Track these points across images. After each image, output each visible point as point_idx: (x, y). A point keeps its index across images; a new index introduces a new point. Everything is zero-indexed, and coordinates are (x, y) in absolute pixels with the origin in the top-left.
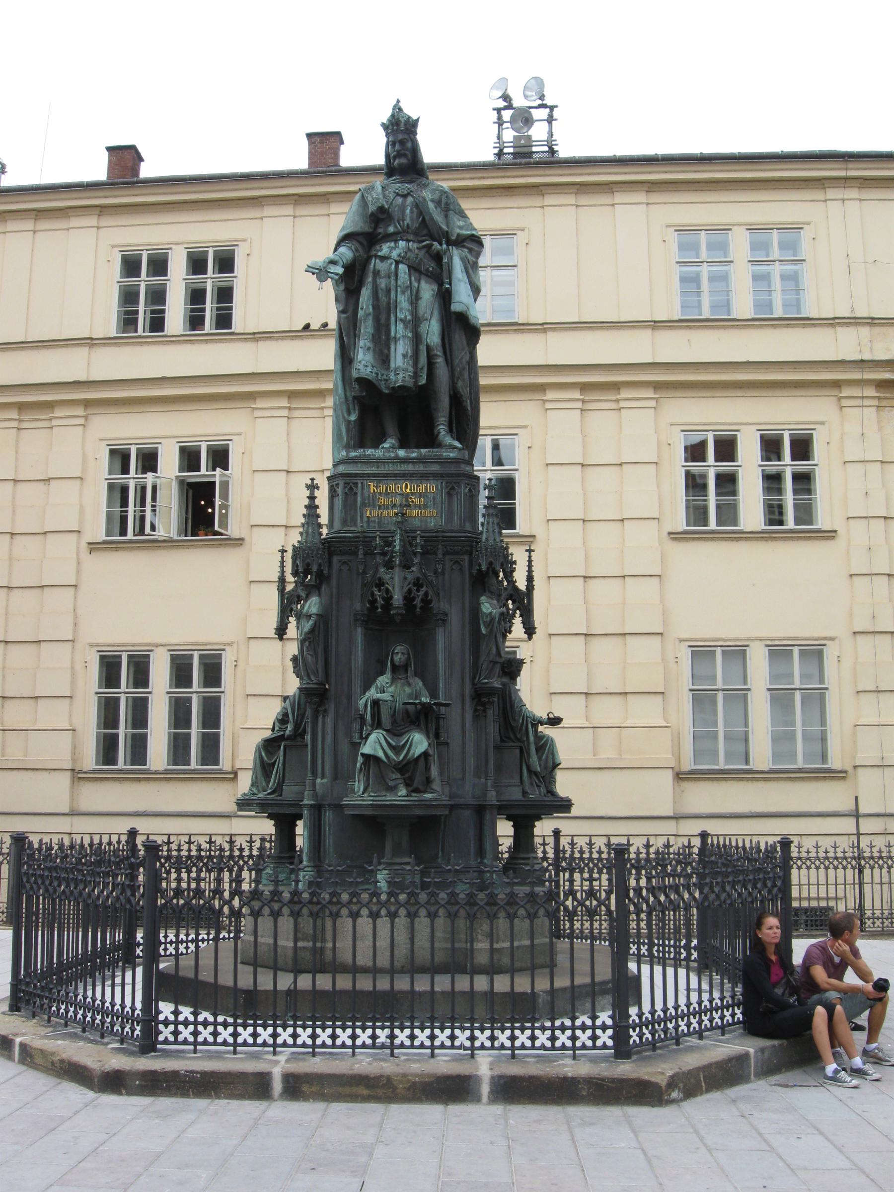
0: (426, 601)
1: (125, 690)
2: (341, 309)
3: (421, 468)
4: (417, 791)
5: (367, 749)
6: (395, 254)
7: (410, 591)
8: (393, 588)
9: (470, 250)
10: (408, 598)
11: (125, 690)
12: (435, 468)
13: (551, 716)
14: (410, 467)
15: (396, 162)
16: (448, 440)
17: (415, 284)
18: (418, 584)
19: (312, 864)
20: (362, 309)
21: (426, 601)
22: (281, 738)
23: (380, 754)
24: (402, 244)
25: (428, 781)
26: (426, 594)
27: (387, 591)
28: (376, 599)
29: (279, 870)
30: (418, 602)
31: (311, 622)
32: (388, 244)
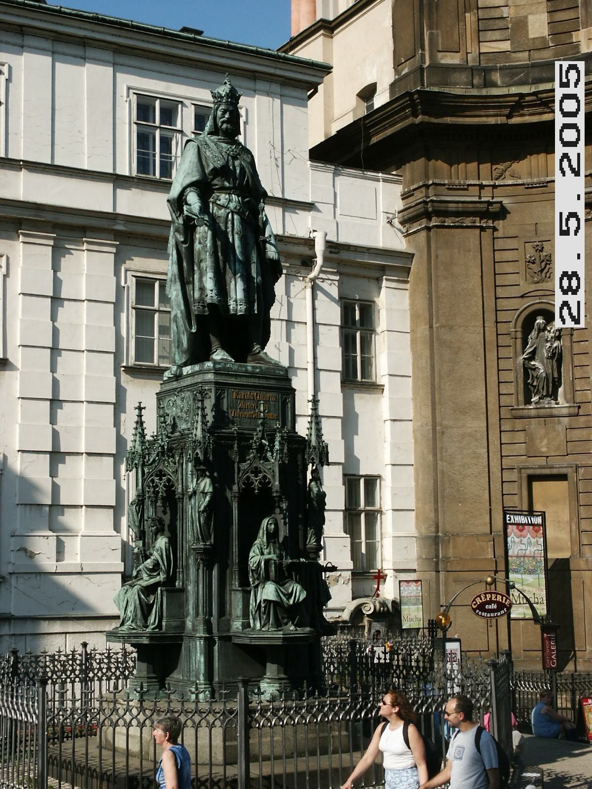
2: (182, 239)
3: (263, 382)
6: (232, 205)
8: (274, 476)
12: (273, 383)
13: (329, 565)
14: (256, 382)
15: (224, 126)
19: (207, 682)
20: (200, 243)
22: (157, 584)
24: (234, 197)
27: (265, 477)
28: (252, 483)
29: (151, 688)
31: (208, 499)
32: (223, 195)
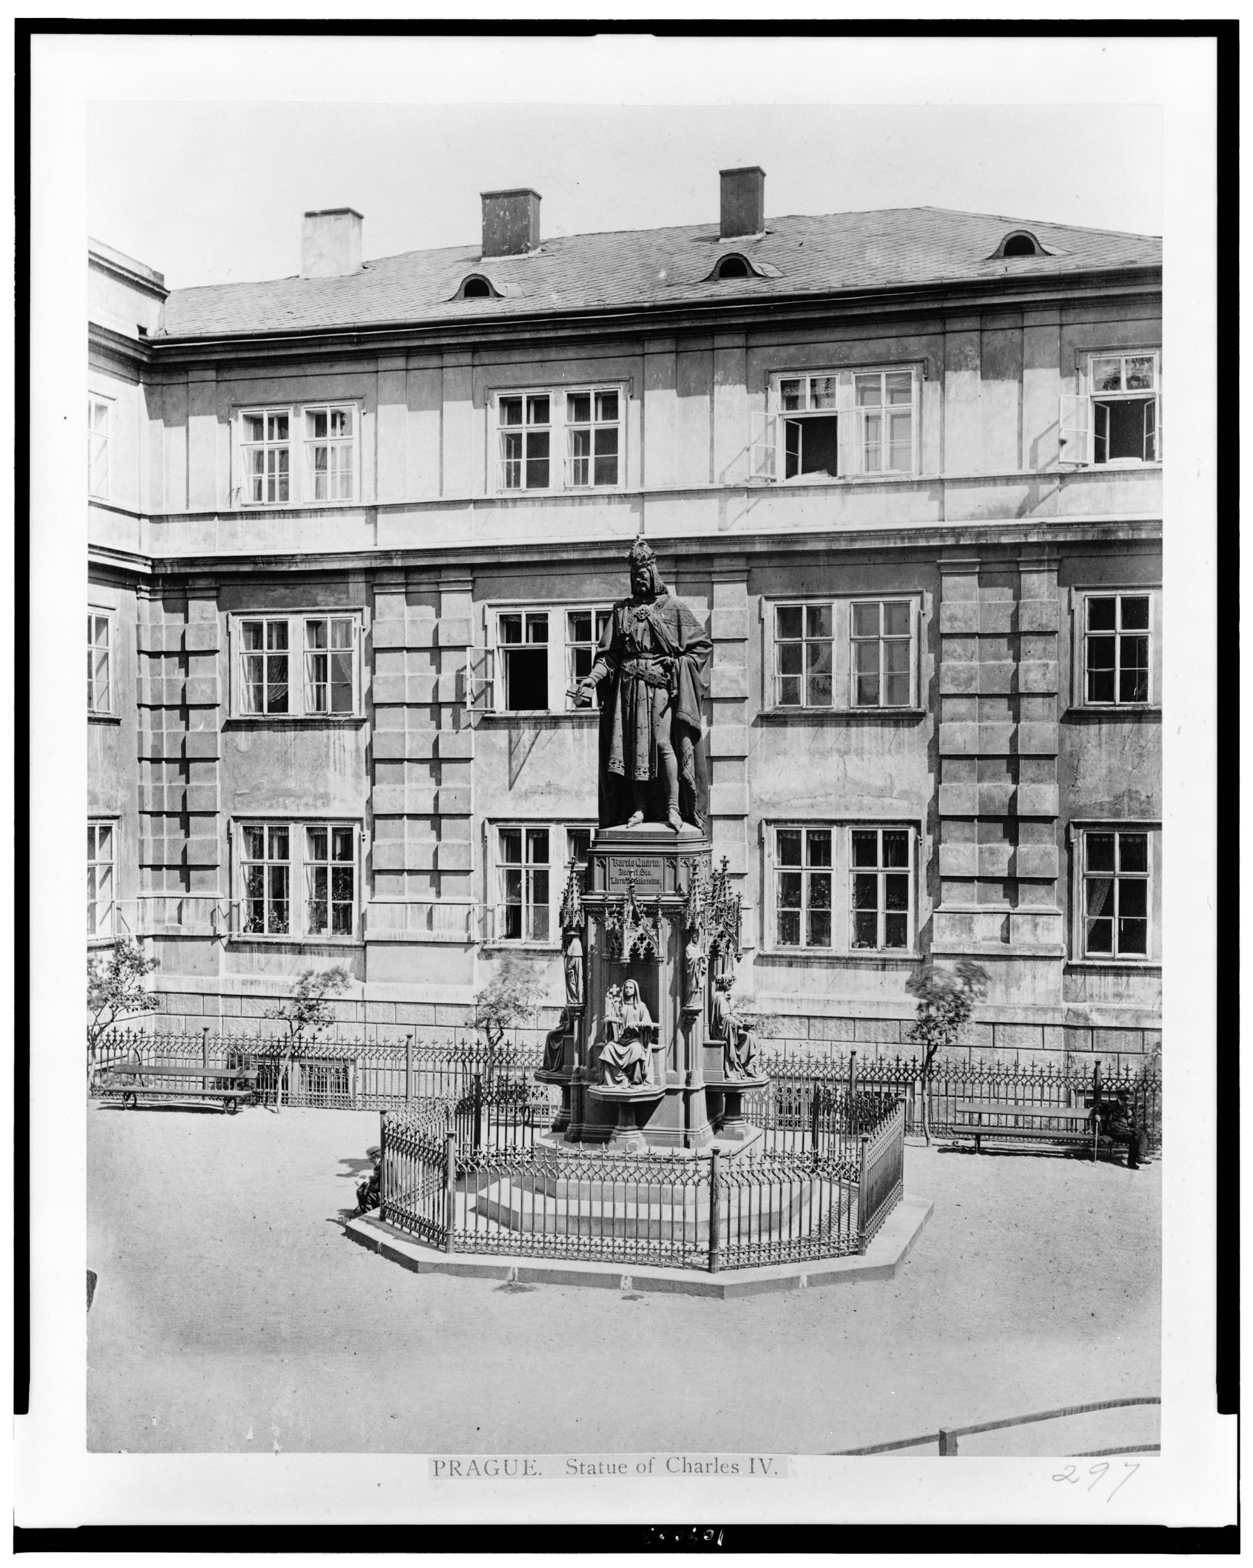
0: (649, 950)
1: (527, 865)
4: (636, 1084)
5: (602, 1057)
7: (635, 944)
9: (699, 654)
10: (634, 950)
11: (527, 865)
16: (675, 817)
17: (651, 695)
18: (642, 938)
21: (649, 950)
23: (611, 1061)
25: (644, 1077)
26: (649, 944)
30: (642, 951)
